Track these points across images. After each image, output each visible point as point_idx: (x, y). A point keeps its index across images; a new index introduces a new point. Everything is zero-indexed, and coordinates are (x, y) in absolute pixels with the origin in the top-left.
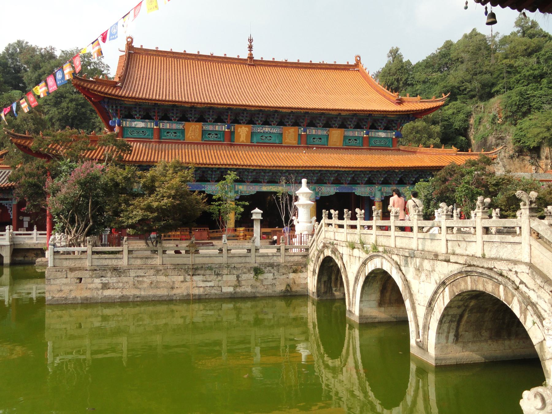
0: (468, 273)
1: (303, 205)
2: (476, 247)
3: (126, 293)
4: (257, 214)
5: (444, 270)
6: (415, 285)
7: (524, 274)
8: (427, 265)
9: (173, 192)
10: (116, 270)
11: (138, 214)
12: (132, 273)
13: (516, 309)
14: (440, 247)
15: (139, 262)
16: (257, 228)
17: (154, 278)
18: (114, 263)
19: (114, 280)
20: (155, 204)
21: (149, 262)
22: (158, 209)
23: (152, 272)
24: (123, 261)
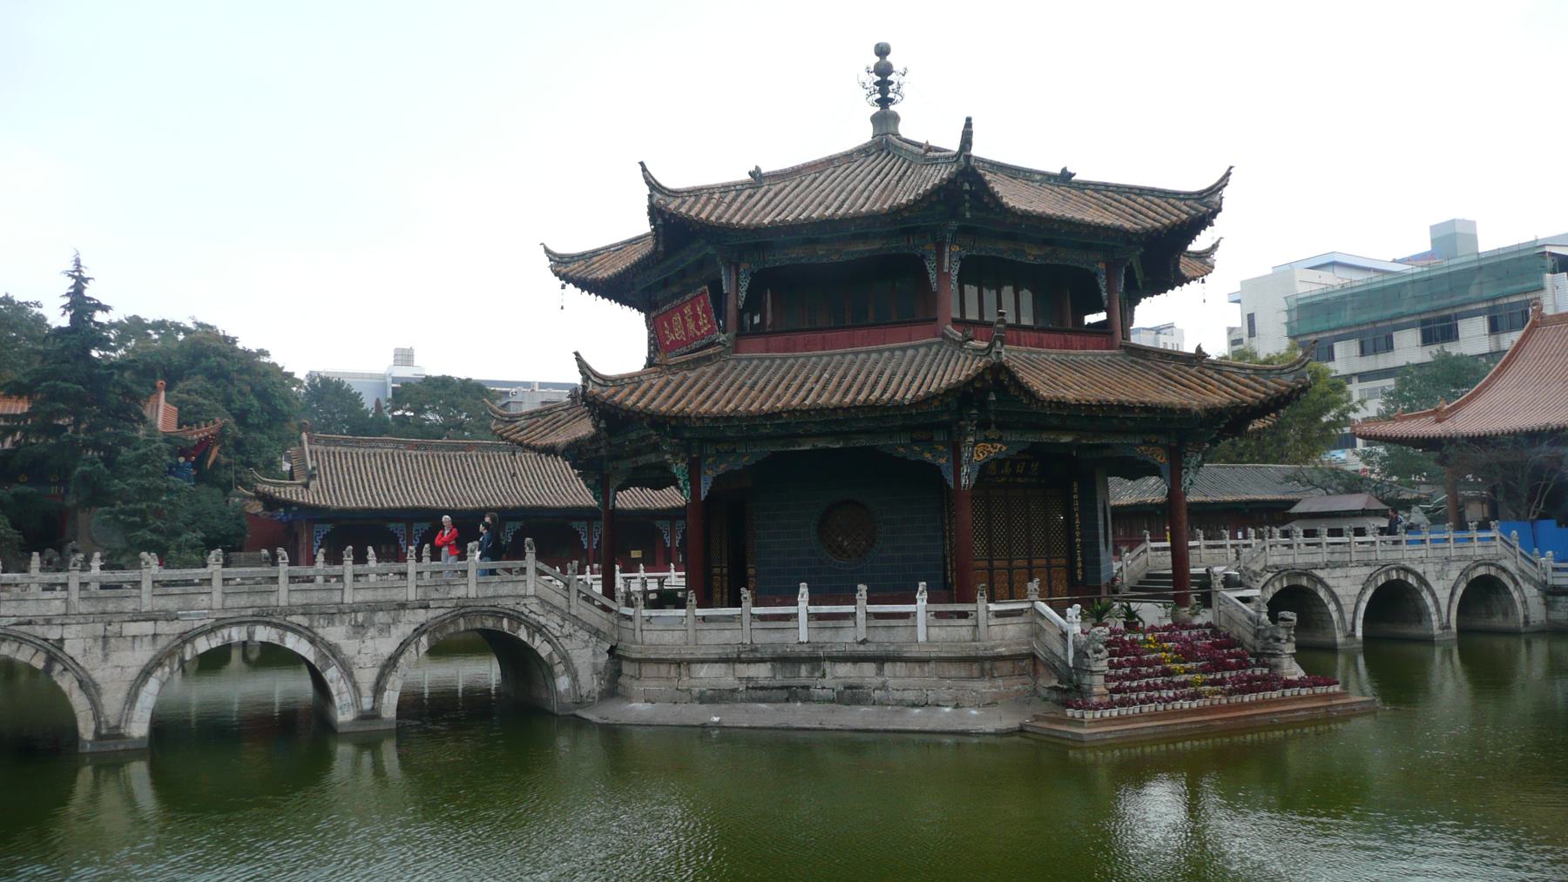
0: (463, 615)
2: (470, 589)
5: (422, 616)
6: (349, 647)
7: (533, 605)
8: (381, 617)
13: (523, 635)
14: (412, 594)
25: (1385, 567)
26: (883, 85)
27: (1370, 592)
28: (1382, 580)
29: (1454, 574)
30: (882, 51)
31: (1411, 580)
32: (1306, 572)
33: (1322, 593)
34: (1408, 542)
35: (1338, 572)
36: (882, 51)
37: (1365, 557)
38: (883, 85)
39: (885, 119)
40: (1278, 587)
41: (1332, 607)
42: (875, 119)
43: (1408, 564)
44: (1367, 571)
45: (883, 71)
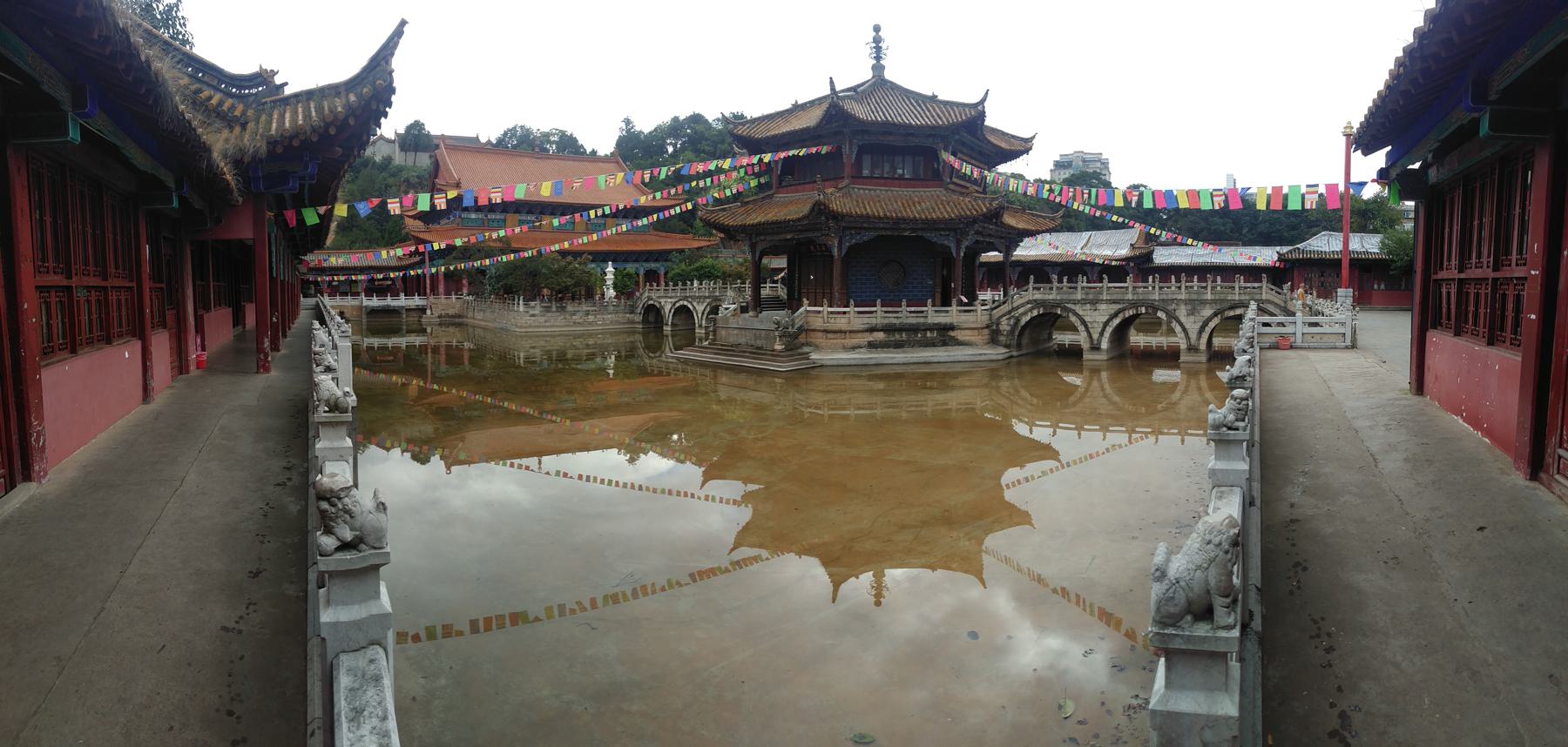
26: (878, 49)
30: (877, 29)
32: (1058, 304)
33: (1073, 319)
36: (877, 29)
37: (1119, 297)
38: (878, 49)
39: (878, 68)
40: (1035, 313)
42: (874, 67)
44: (1117, 307)
45: (877, 40)
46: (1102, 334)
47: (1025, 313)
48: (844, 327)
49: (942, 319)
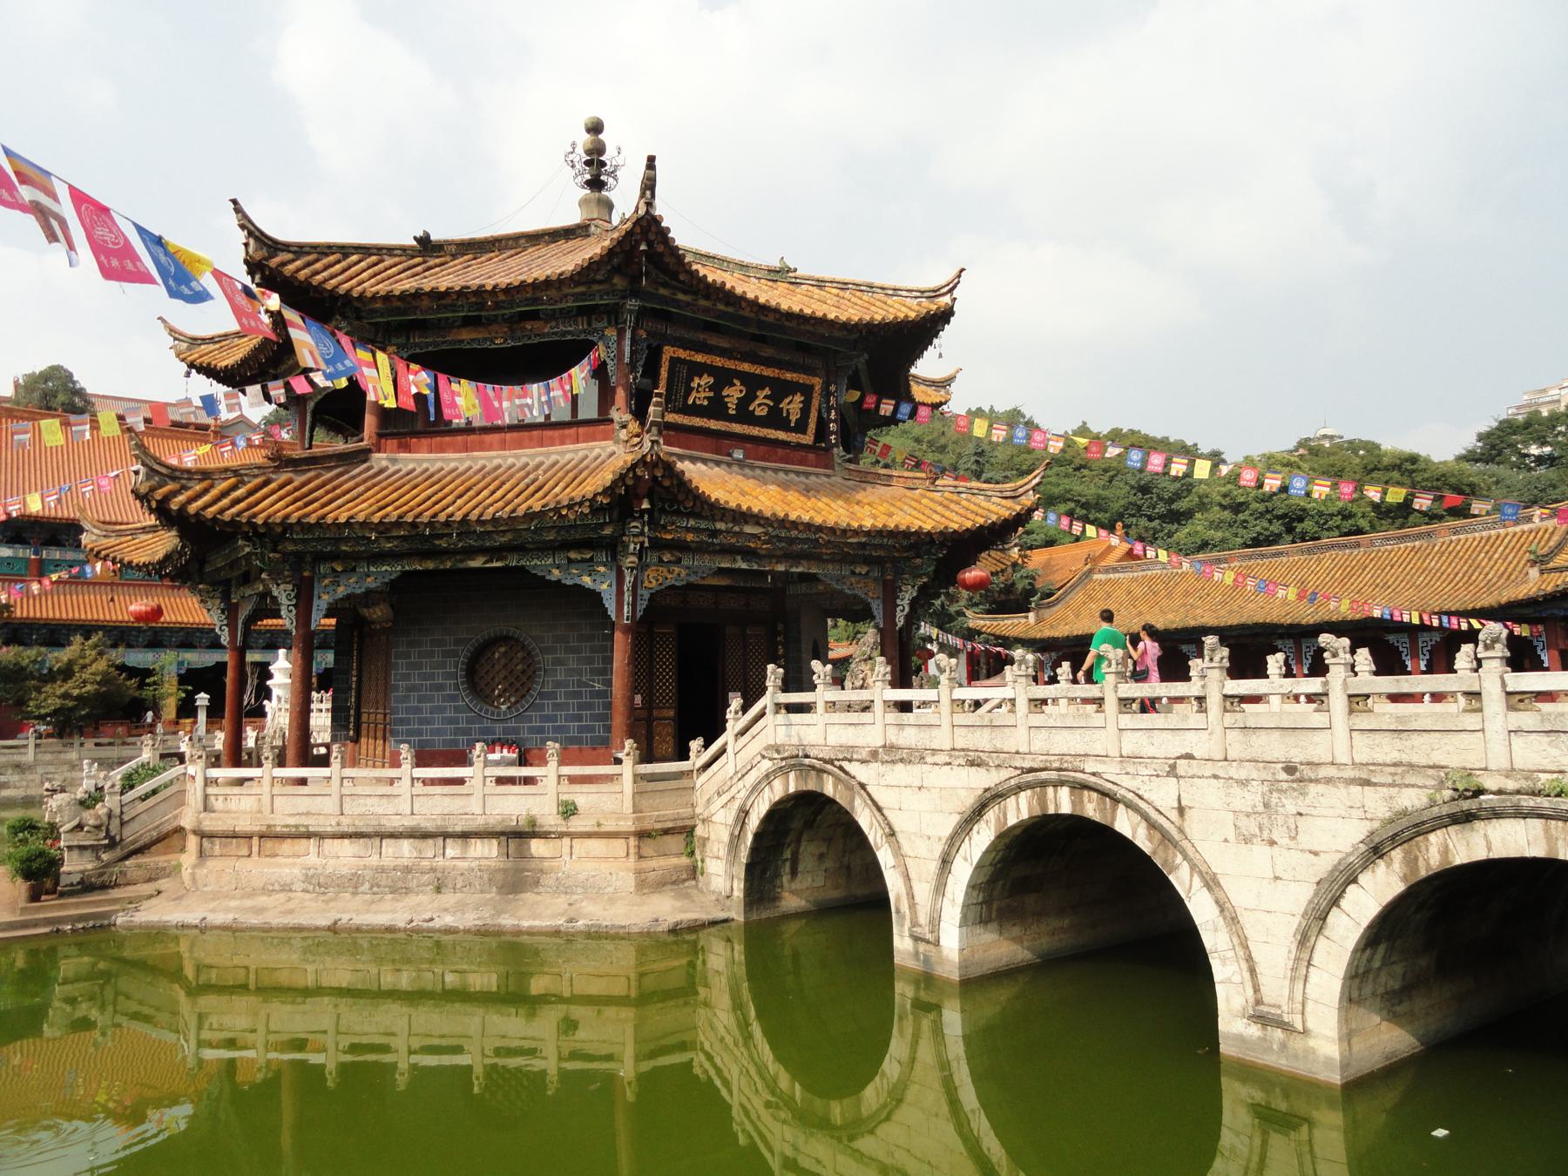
1: (280, 686)
3: (31, 792)
4: (203, 699)
9: (98, 678)
10: (18, 767)
11: (54, 703)
12: (40, 770)
15: (48, 757)
16: (202, 716)
17: (68, 775)
18: (17, 758)
19: (16, 778)
20: (76, 692)
21: (62, 756)
22: (79, 698)
23: (66, 767)
24: (29, 756)
25: (1034, 780)
27: (983, 837)
28: (1019, 810)
29: (1338, 824)
31: (1124, 824)
32: (834, 764)
33: (864, 818)
34: (832, 706)
35: (900, 773)
36: (596, 128)
37: (982, 740)
41: (885, 857)
43: (1109, 772)
46: (940, 887)
47: (756, 789)
48: (244, 825)
49: (512, 806)
